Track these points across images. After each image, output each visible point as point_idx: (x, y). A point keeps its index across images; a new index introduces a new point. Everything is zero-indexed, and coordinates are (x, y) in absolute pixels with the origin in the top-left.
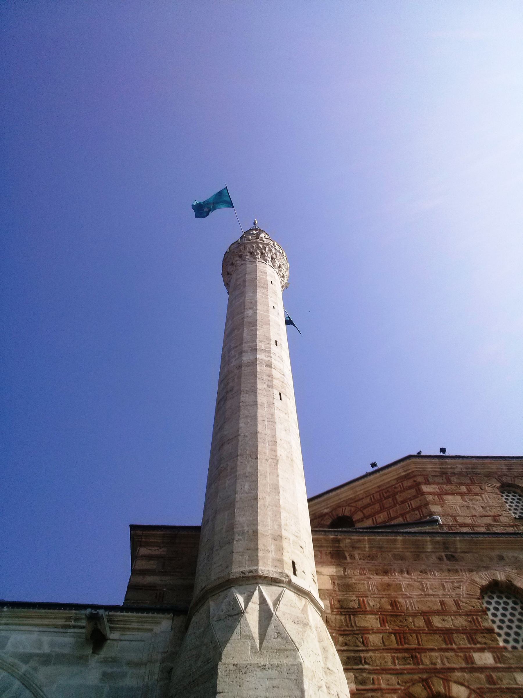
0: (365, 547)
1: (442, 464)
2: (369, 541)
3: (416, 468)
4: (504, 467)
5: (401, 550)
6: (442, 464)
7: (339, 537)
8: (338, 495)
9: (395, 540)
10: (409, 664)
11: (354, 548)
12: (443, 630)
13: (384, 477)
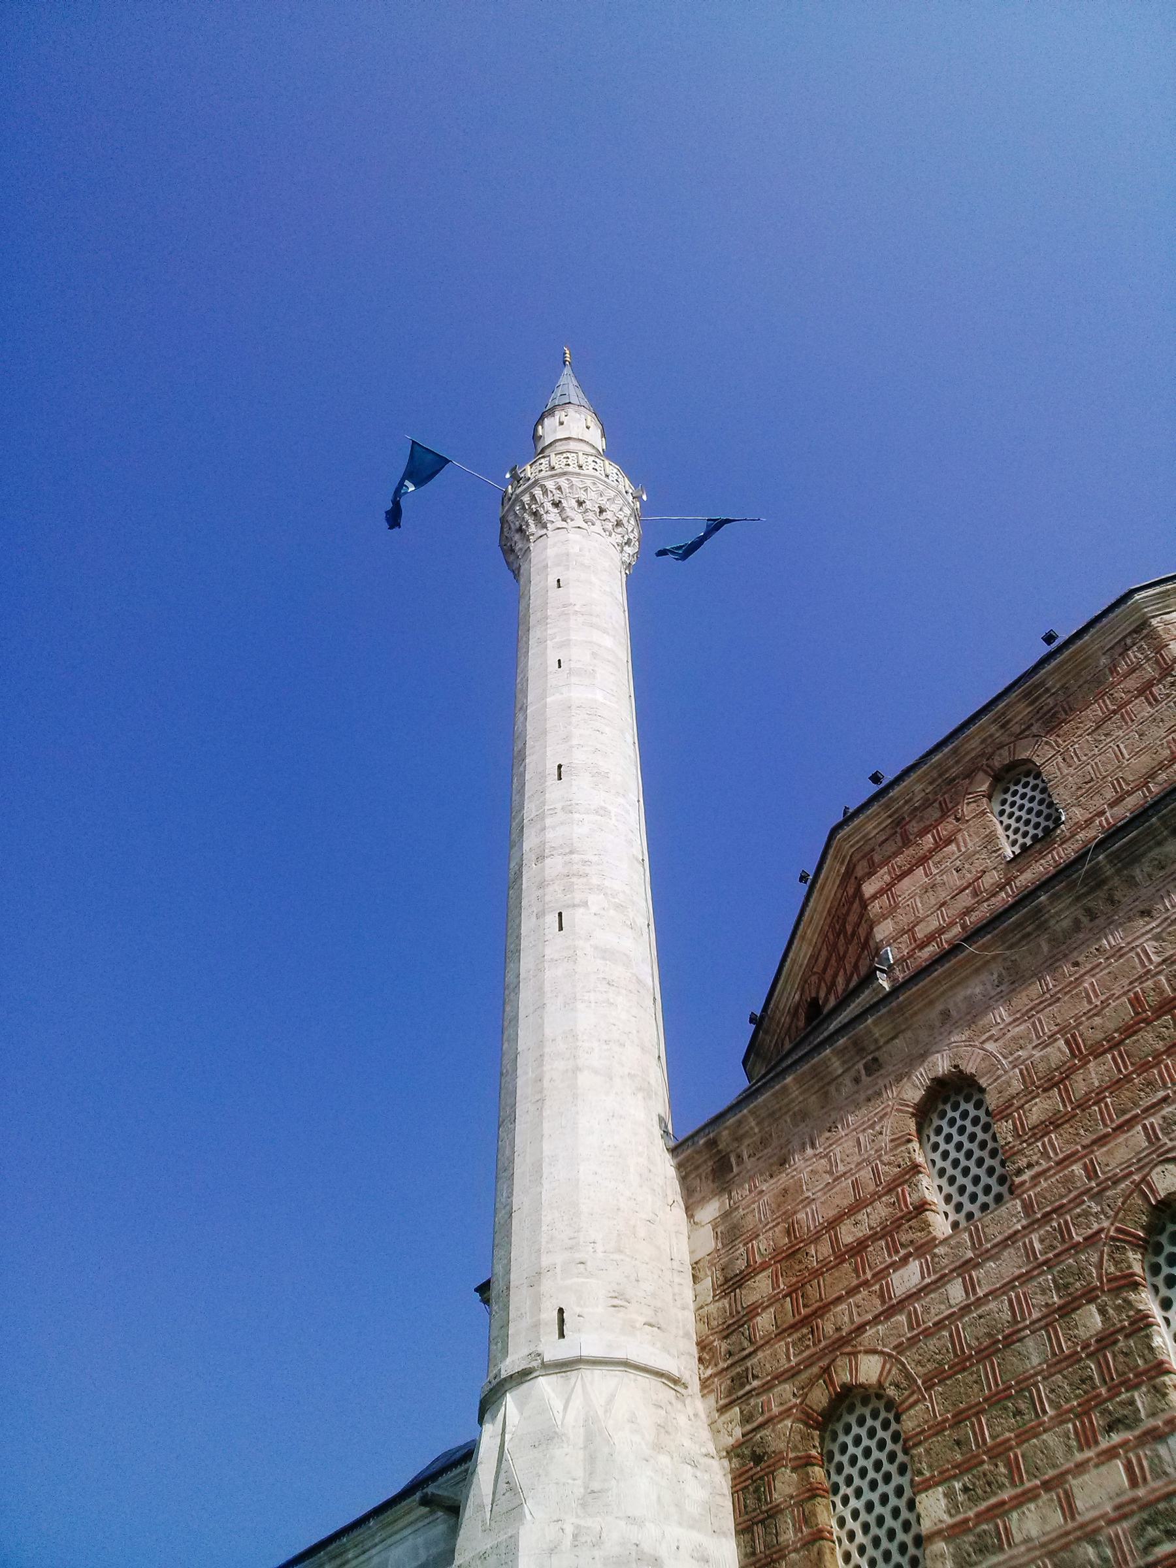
0: (752, 1128)
1: (887, 807)
2: (751, 1112)
3: (852, 846)
4: (993, 728)
5: (801, 1099)
6: (887, 807)
7: (711, 1135)
8: (794, 961)
9: (785, 1089)
10: (808, 1347)
11: (738, 1139)
12: (854, 1248)
13: (826, 891)
